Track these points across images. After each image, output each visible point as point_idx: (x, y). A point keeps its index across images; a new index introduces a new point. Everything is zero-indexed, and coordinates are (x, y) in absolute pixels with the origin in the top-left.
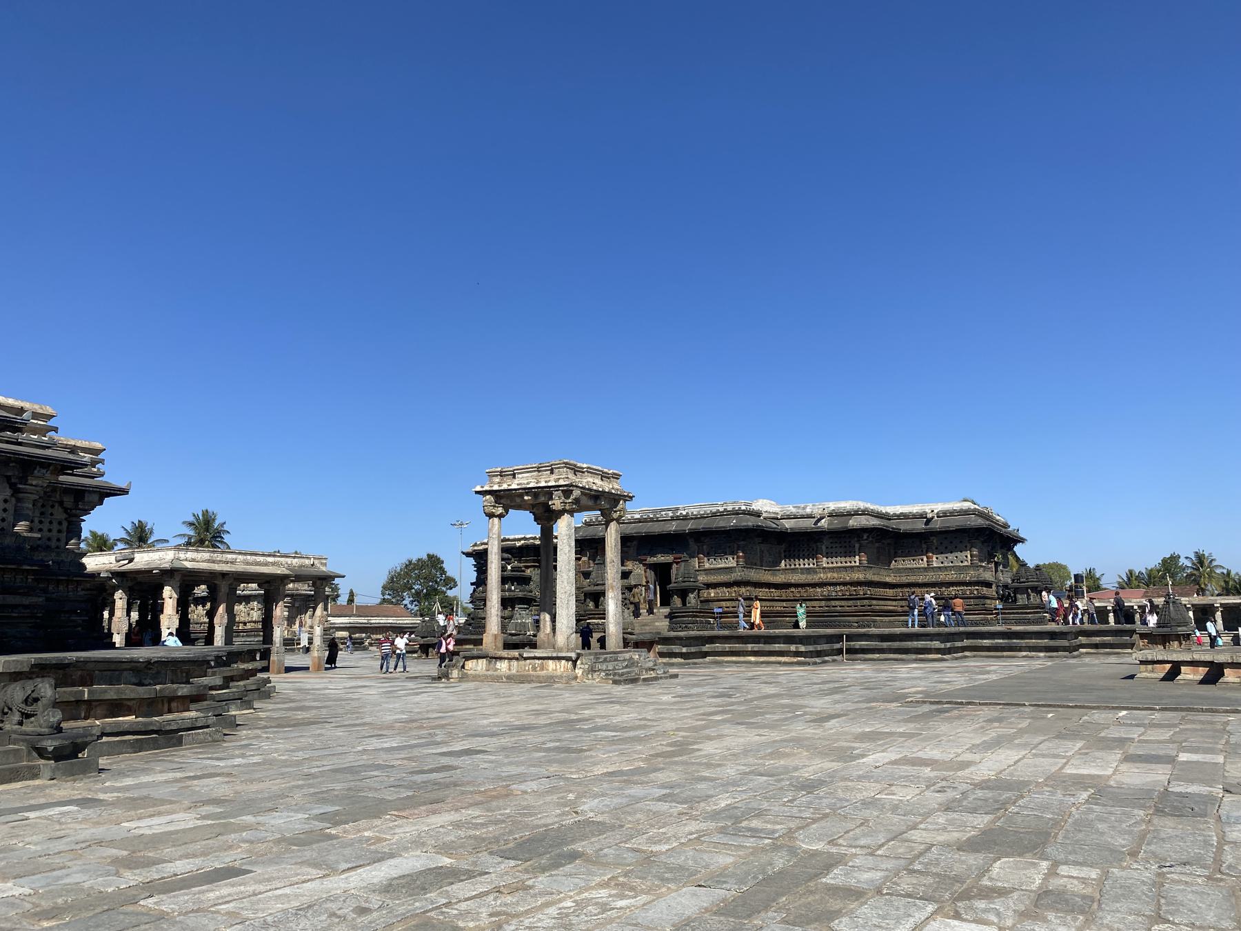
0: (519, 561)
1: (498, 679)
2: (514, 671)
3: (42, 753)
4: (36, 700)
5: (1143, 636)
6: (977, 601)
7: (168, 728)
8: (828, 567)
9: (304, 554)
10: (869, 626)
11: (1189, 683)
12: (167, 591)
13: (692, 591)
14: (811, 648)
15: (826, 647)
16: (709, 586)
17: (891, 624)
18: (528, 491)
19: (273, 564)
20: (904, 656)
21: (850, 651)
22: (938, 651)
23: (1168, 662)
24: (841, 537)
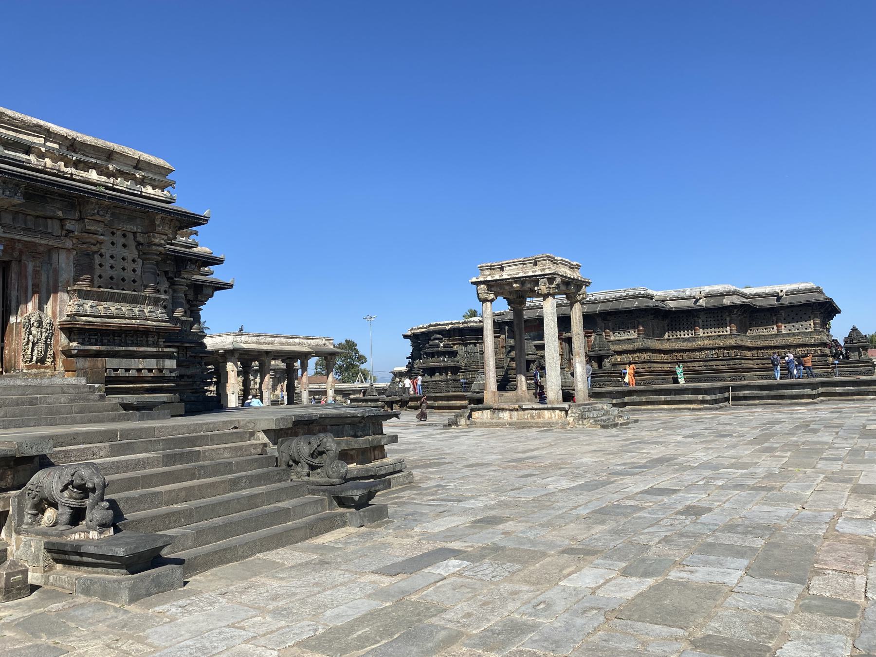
0: (448, 340)
1: (502, 425)
2: (515, 419)
3: (343, 502)
4: (321, 453)
6: (820, 358)
8: (704, 336)
9: (317, 336)
10: (740, 380)
12: (230, 366)
13: (607, 357)
14: (713, 397)
15: (719, 396)
16: (620, 353)
17: (752, 378)
18: (517, 280)
19: (299, 344)
20: (780, 401)
21: (734, 399)
24: (716, 313)
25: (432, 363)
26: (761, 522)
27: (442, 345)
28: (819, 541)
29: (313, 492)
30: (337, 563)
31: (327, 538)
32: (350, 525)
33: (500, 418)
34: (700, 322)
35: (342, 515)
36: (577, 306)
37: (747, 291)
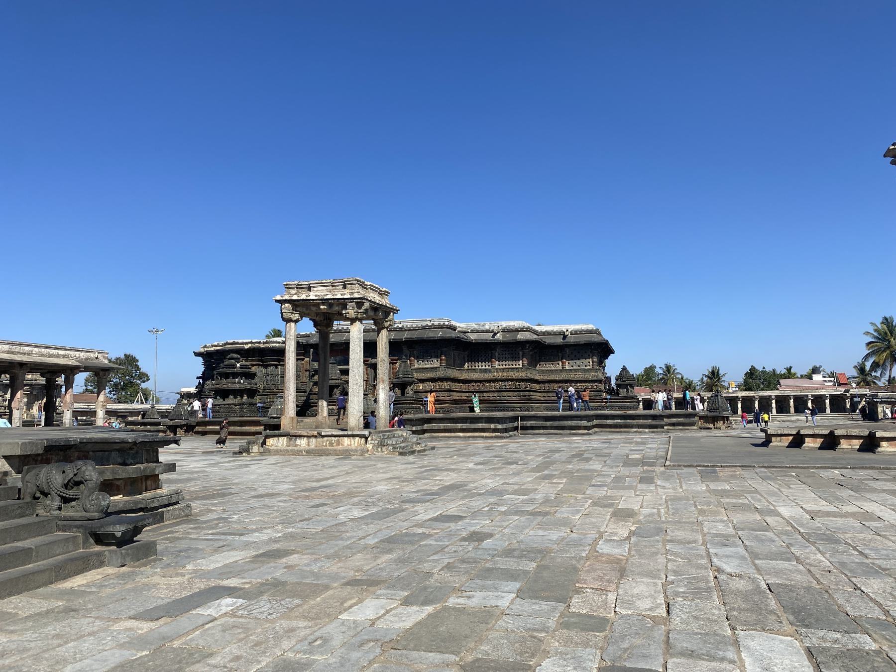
0: (246, 360)
1: (299, 453)
3: (100, 539)
5: (701, 418)
6: (596, 393)
7: (153, 505)
8: (499, 368)
10: (529, 411)
11: (811, 449)
13: (410, 384)
14: (504, 426)
15: (509, 425)
16: (422, 381)
17: (539, 409)
18: (324, 301)
19: (64, 356)
21: (524, 428)
22: (586, 428)
23: (791, 435)
24: (511, 347)
25: (226, 384)
26: (535, 545)
27: (238, 365)
28: (582, 562)
29: (64, 529)
30: (86, 610)
31: (77, 582)
32: (109, 565)
33: (296, 445)
34: (497, 354)
35: (99, 554)
36: (384, 333)
37: (538, 328)
